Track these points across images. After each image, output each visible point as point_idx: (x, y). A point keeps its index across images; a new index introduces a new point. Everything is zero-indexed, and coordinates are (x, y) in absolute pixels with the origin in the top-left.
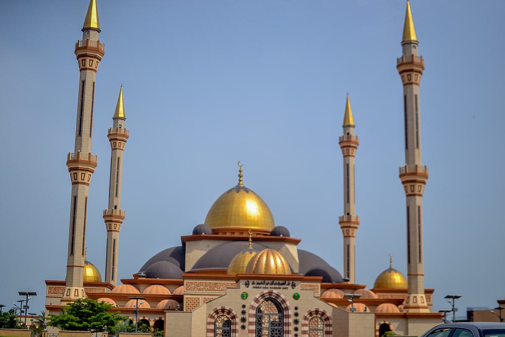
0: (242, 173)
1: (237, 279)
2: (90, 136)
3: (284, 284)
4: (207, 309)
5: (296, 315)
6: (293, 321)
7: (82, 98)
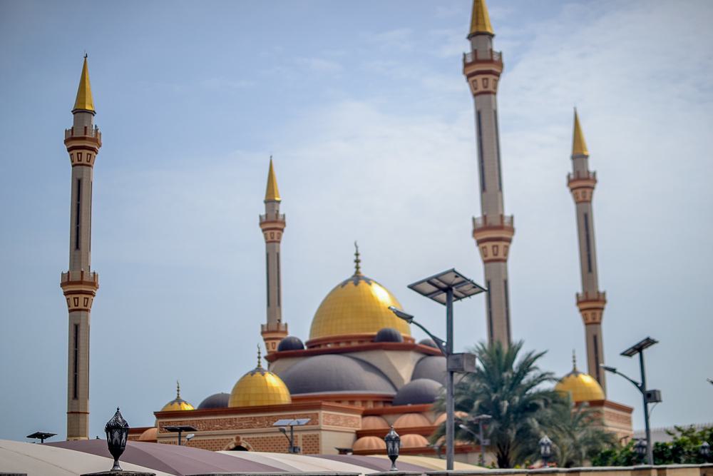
0: (360, 258)
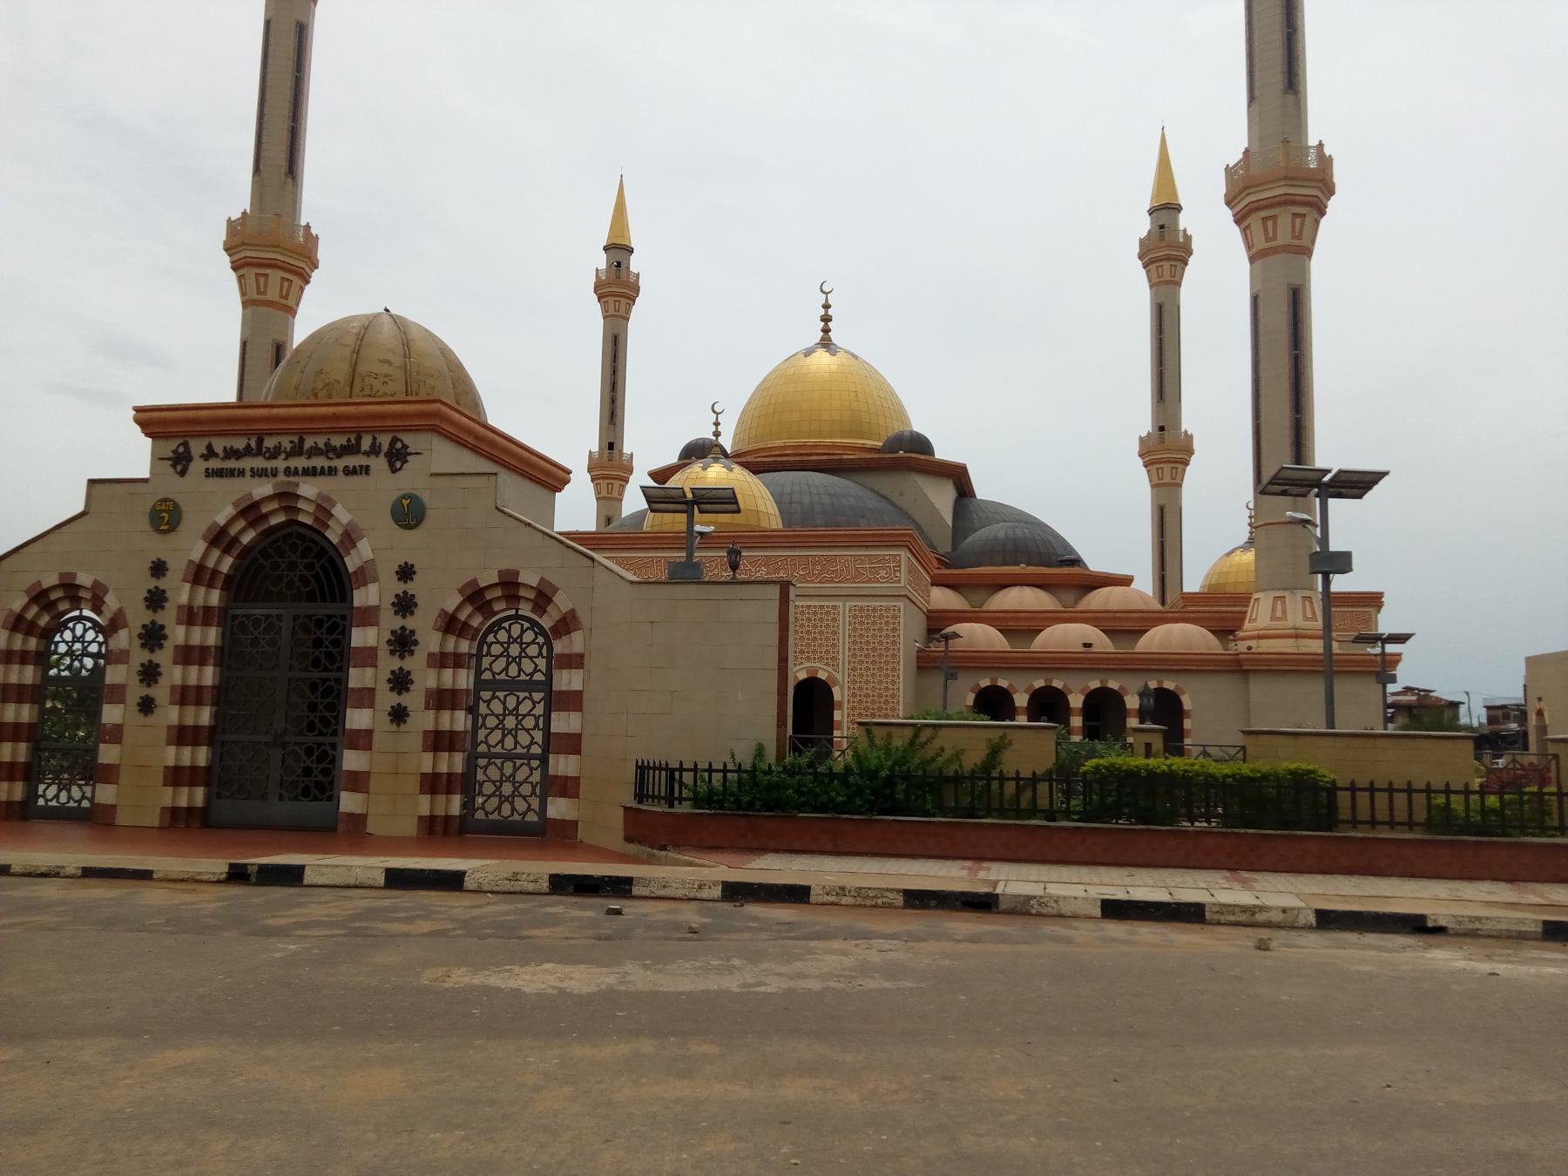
3: (351, 449)
5: (405, 605)
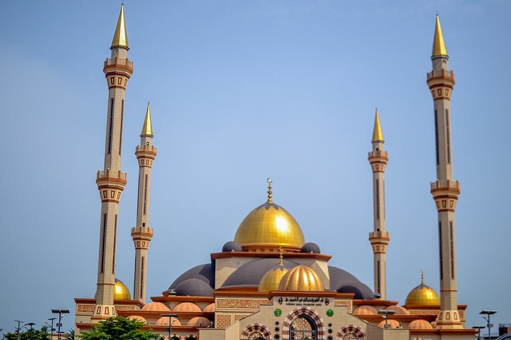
1: (270, 296)
2: (120, 154)
4: (241, 326)
5: (330, 331)
6: (327, 337)
7: (111, 116)
